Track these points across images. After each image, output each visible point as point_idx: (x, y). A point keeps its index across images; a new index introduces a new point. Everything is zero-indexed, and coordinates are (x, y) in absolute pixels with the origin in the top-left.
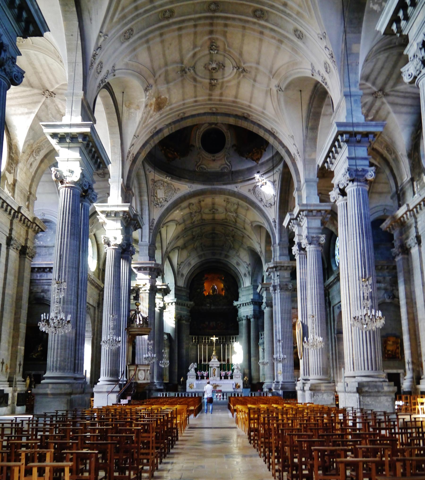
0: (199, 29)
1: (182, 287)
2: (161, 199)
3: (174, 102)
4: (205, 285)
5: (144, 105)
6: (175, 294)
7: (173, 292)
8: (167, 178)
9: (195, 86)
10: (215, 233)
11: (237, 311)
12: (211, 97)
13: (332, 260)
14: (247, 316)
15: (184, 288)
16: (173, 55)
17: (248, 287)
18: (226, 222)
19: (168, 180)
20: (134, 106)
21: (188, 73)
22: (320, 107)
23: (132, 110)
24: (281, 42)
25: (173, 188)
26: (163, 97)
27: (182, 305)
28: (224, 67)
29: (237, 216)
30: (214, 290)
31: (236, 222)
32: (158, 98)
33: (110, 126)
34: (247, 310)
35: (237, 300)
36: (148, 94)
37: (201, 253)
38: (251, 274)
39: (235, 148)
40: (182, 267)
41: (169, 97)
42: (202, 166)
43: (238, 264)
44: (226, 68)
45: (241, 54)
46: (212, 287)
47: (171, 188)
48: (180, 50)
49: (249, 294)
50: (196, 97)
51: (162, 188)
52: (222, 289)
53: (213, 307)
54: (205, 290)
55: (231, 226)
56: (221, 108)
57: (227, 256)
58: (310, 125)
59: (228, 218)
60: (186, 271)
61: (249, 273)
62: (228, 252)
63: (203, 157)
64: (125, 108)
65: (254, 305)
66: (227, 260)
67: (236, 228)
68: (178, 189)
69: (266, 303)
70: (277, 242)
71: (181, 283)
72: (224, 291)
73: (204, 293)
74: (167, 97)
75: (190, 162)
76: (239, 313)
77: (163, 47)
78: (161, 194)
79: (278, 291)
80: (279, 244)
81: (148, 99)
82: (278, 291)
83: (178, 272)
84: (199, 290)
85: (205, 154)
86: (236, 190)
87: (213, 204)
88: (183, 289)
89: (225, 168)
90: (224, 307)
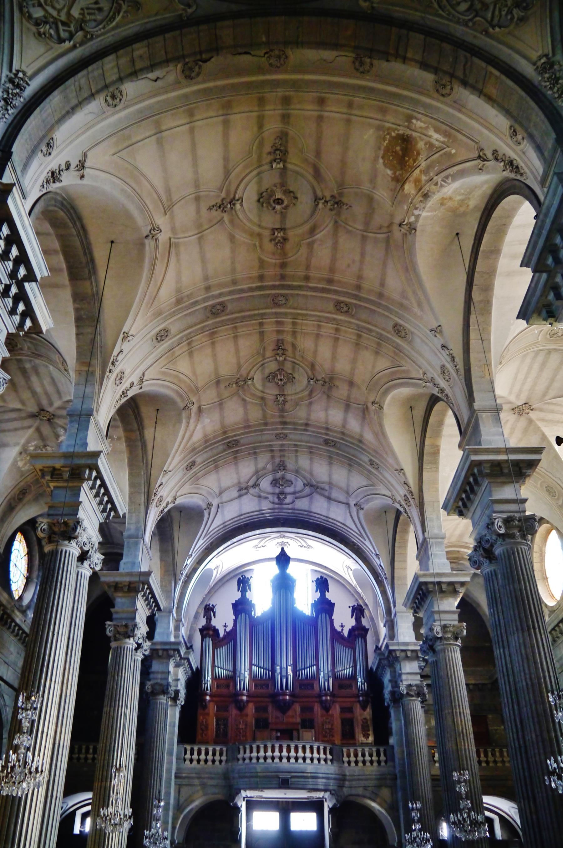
0: (301, 273)
3: (371, 131)
9: (318, 154)
16: (349, 246)
21: (328, 195)
24: (179, 301)
26: (389, 172)
28: (259, 201)
36: (412, 219)
41: (376, 160)
44: (256, 198)
45: (232, 238)
48: (335, 247)
56: (260, 70)
74: (381, 161)
77: (360, 269)
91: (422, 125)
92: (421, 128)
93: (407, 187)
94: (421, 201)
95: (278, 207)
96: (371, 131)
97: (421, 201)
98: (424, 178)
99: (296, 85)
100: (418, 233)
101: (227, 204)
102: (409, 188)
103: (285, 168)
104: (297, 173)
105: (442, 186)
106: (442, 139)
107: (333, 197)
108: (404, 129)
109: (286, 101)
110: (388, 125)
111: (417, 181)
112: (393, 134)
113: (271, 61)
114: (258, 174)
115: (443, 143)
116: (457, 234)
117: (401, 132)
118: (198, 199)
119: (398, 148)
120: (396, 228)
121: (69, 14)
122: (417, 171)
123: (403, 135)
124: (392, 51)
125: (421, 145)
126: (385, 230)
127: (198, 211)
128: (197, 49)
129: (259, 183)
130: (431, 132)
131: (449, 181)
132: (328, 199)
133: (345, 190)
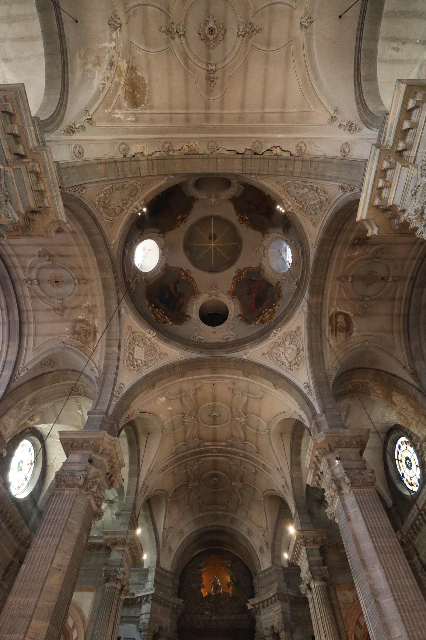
1: (167, 571)
2: (139, 362)
4: (203, 576)
5: (107, 57)
6: (155, 581)
7: (151, 577)
8: (152, 332)
10: (216, 475)
11: (253, 622)
12: (208, 112)
13: (399, 486)
14: (272, 627)
15: (171, 573)
17: (268, 570)
18: (231, 445)
19: (150, 335)
20: (92, 58)
22: (374, 38)
23: (89, 66)
25: (158, 351)
26: (139, 74)
27: (164, 605)
28: (225, 31)
29: (247, 423)
30: (217, 587)
31: (246, 440)
32: (132, 69)
33: (49, 79)
34: (271, 614)
35: (253, 596)
37: (197, 516)
38: (270, 546)
39: (240, 318)
40: (170, 536)
41: (150, 81)
42: (199, 337)
43: (250, 532)
44: (228, 34)
46: (215, 582)
47: (156, 351)
49: (272, 583)
50: (187, 109)
51: (142, 345)
52: (229, 585)
53: (214, 618)
54: (203, 587)
55: (238, 454)
57: (233, 520)
58: (362, 73)
59: (235, 433)
60: (176, 544)
61: (267, 544)
62: (235, 513)
63: (200, 329)
64: (79, 61)
65: (281, 600)
66: (234, 527)
67: (246, 457)
68: (166, 354)
69: (310, 570)
70: (318, 411)
71: (167, 564)
72: (231, 588)
73: (202, 590)
74: (146, 82)
75: (184, 329)
76: (258, 625)
78: (139, 353)
79: (346, 490)
80: (324, 411)
81: (114, 48)
82: (346, 490)
83: (164, 543)
84: (194, 585)
85: (203, 326)
86: (245, 357)
87: (214, 400)
88: (168, 575)
89: (228, 338)
90: (233, 617)
91: (128, 119)
92: (128, 117)
93: (126, 65)
94: (113, 57)
95: (211, 25)
96: (156, 104)
97: (113, 57)
98: (117, 80)
99: (201, 129)
100: (107, 21)
101: (249, 31)
102: (123, 65)
103: (208, 64)
104: (200, 60)
105: (104, 80)
106: (115, 115)
107: (173, 39)
108: (137, 112)
109: (207, 118)
110: (148, 112)
111: (120, 75)
112: (143, 105)
113: (215, 145)
114: (225, 59)
115: (113, 114)
116: (77, 21)
117: (139, 109)
118: (269, 44)
119: (138, 96)
120: (123, 20)
121: (309, 191)
122: (122, 83)
123: (137, 107)
124: (155, 161)
125: (125, 104)
126: (131, 12)
127: (270, 29)
128: (253, 160)
129: (225, 50)
130: (122, 117)
131: (101, 86)
132: (176, 34)
133: (165, 47)
